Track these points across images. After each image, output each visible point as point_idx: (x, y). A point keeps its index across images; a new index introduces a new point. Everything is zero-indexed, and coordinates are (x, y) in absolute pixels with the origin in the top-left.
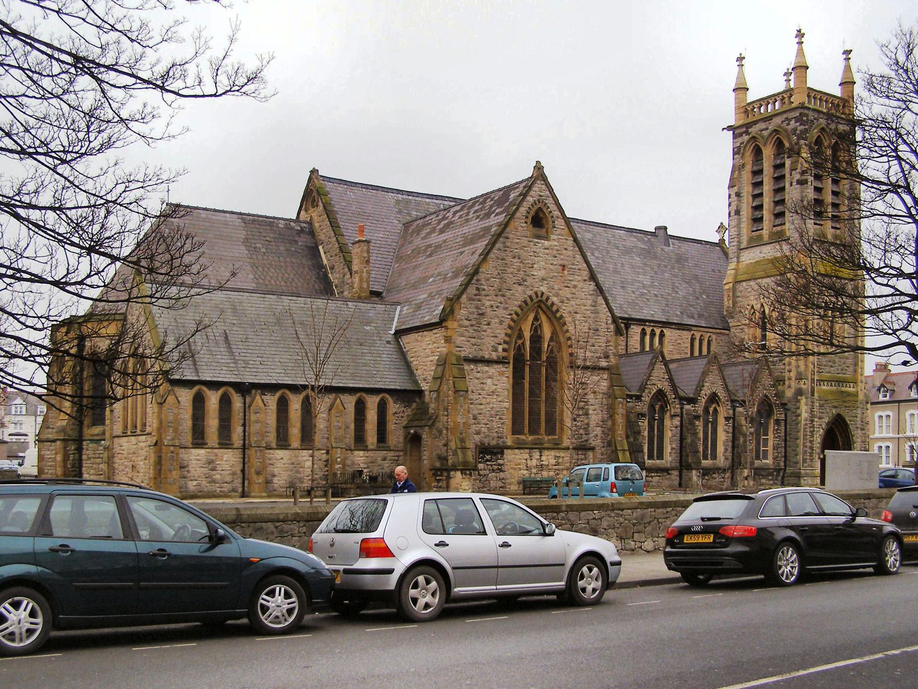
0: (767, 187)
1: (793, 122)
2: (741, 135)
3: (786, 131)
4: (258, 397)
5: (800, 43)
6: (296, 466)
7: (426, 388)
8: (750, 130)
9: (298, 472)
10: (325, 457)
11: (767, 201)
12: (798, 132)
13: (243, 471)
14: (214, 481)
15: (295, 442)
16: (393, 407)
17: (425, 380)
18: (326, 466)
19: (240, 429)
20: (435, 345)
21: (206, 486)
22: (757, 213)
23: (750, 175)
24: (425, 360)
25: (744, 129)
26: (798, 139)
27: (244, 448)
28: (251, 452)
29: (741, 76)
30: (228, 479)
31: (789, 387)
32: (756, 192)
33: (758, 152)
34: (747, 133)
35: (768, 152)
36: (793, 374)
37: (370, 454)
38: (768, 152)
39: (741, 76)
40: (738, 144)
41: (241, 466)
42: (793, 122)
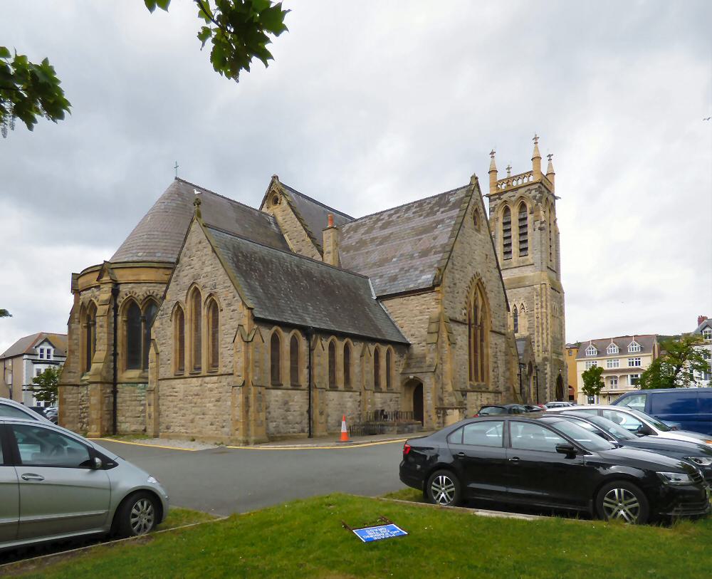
0: (515, 233)
1: (534, 191)
2: (495, 200)
3: (529, 197)
4: (319, 341)
5: (536, 143)
6: (342, 405)
7: (414, 342)
8: (502, 197)
9: (343, 412)
10: (359, 398)
11: (515, 240)
12: (537, 198)
13: (309, 412)
14: (288, 423)
15: (341, 385)
16: (395, 357)
17: (412, 335)
18: (359, 406)
19: (306, 371)
20: (424, 307)
21: (284, 429)
22: (507, 248)
23: (502, 224)
24: (412, 319)
25: (497, 196)
26: (538, 202)
27: (310, 388)
28: (315, 393)
29: (493, 163)
30: (298, 419)
31: (538, 356)
32: (506, 235)
33: (507, 210)
34: (499, 198)
35: (514, 211)
36: (540, 348)
37: (384, 395)
38: (514, 211)
39: (493, 163)
40: (493, 206)
41: (307, 406)
42: (534, 191)
